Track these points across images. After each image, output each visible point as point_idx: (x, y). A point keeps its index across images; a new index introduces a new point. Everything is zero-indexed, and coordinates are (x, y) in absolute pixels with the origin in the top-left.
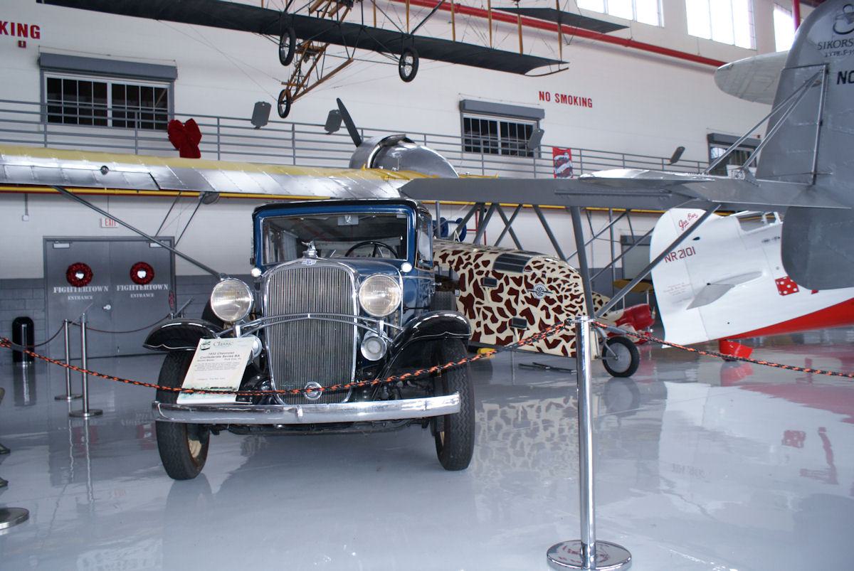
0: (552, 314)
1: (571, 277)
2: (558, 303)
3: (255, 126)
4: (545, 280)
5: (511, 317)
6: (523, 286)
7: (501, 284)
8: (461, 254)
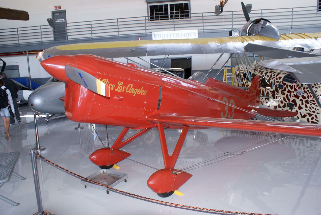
0: (304, 103)
1: (314, 88)
2: (307, 99)
3: (216, 15)
4: (302, 88)
5: (288, 102)
6: (293, 90)
7: (285, 88)
8: (272, 73)
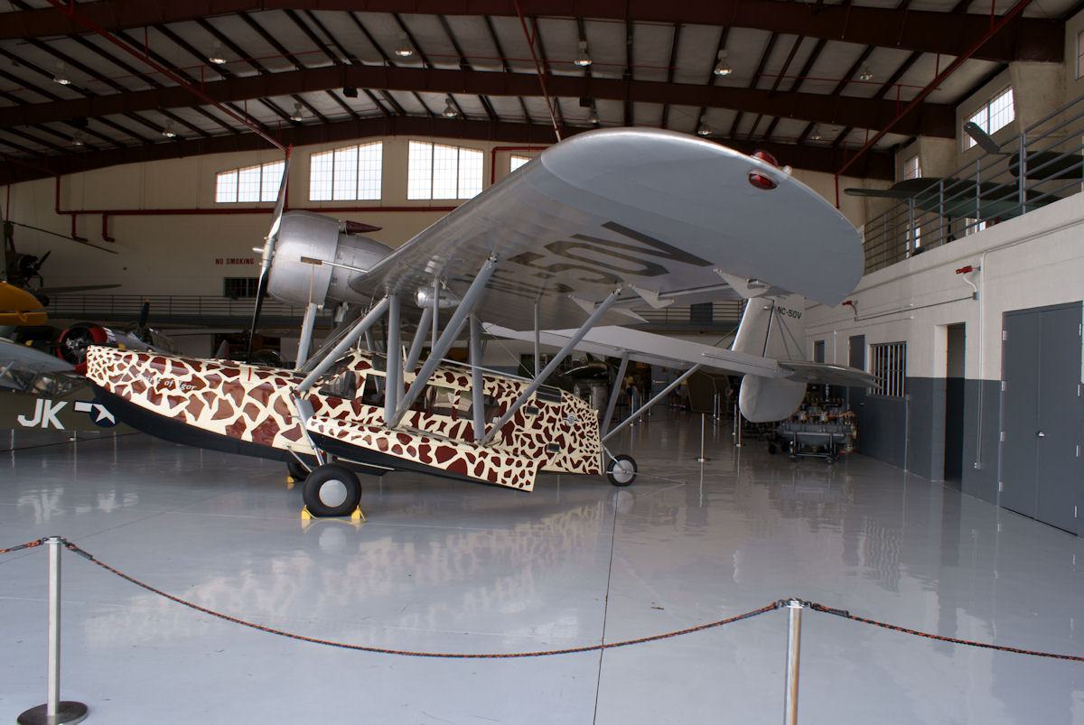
4: (576, 410)
5: (547, 442)
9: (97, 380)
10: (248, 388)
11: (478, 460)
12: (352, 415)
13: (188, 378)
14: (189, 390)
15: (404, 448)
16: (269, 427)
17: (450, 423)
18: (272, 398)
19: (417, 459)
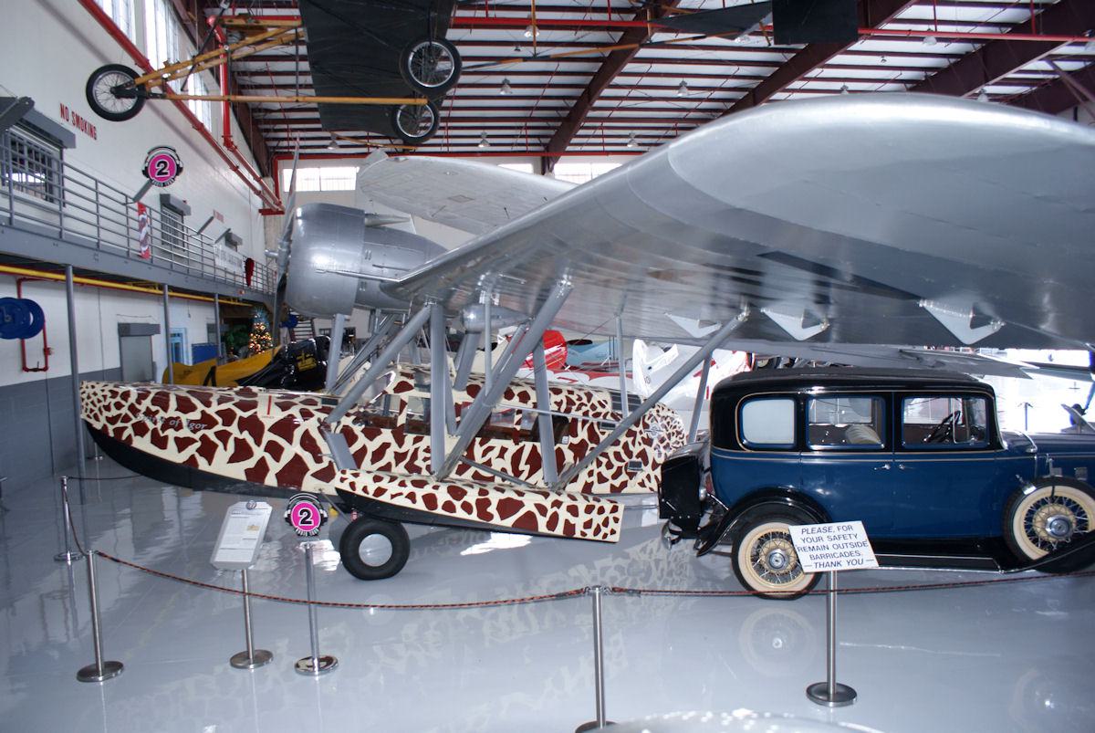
5: (627, 459)
9: (92, 421)
10: (268, 423)
11: (550, 511)
12: (394, 447)
13: (196, 415)
14: (199, 430)
15: (458, 504)
16: (297, 467)
17: (512, 447)
18: (298, 434)
19: (474, 517)
